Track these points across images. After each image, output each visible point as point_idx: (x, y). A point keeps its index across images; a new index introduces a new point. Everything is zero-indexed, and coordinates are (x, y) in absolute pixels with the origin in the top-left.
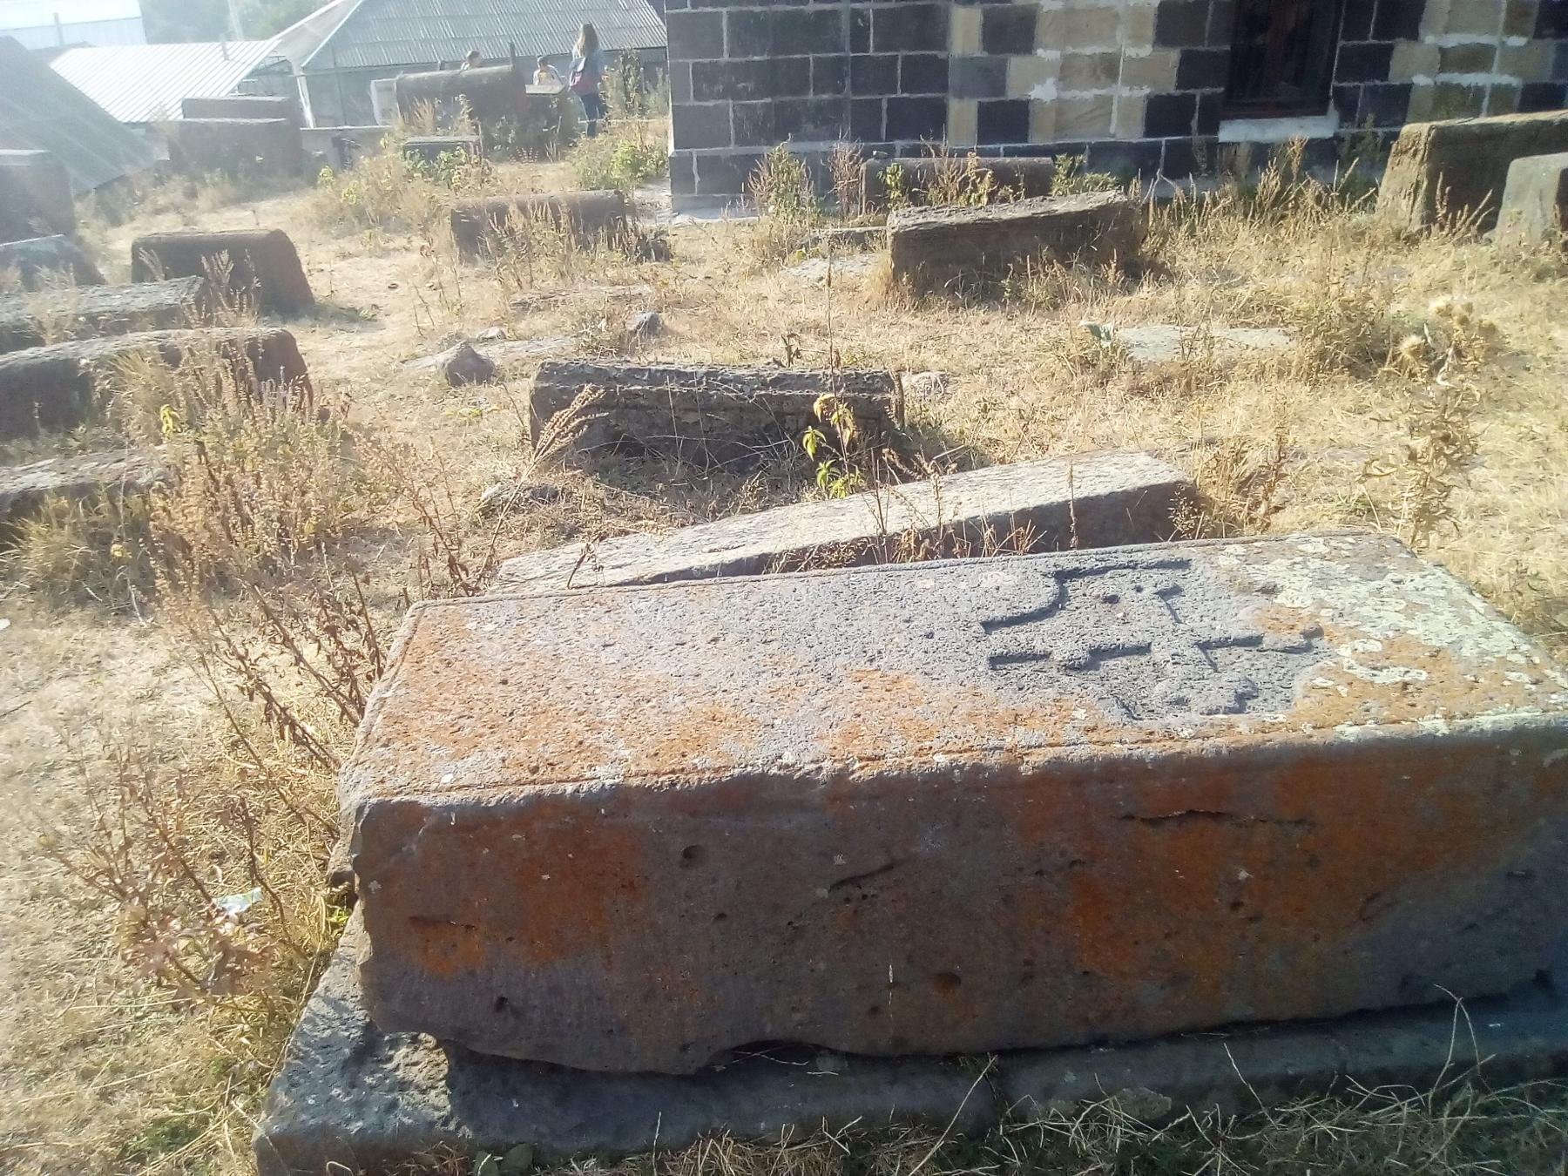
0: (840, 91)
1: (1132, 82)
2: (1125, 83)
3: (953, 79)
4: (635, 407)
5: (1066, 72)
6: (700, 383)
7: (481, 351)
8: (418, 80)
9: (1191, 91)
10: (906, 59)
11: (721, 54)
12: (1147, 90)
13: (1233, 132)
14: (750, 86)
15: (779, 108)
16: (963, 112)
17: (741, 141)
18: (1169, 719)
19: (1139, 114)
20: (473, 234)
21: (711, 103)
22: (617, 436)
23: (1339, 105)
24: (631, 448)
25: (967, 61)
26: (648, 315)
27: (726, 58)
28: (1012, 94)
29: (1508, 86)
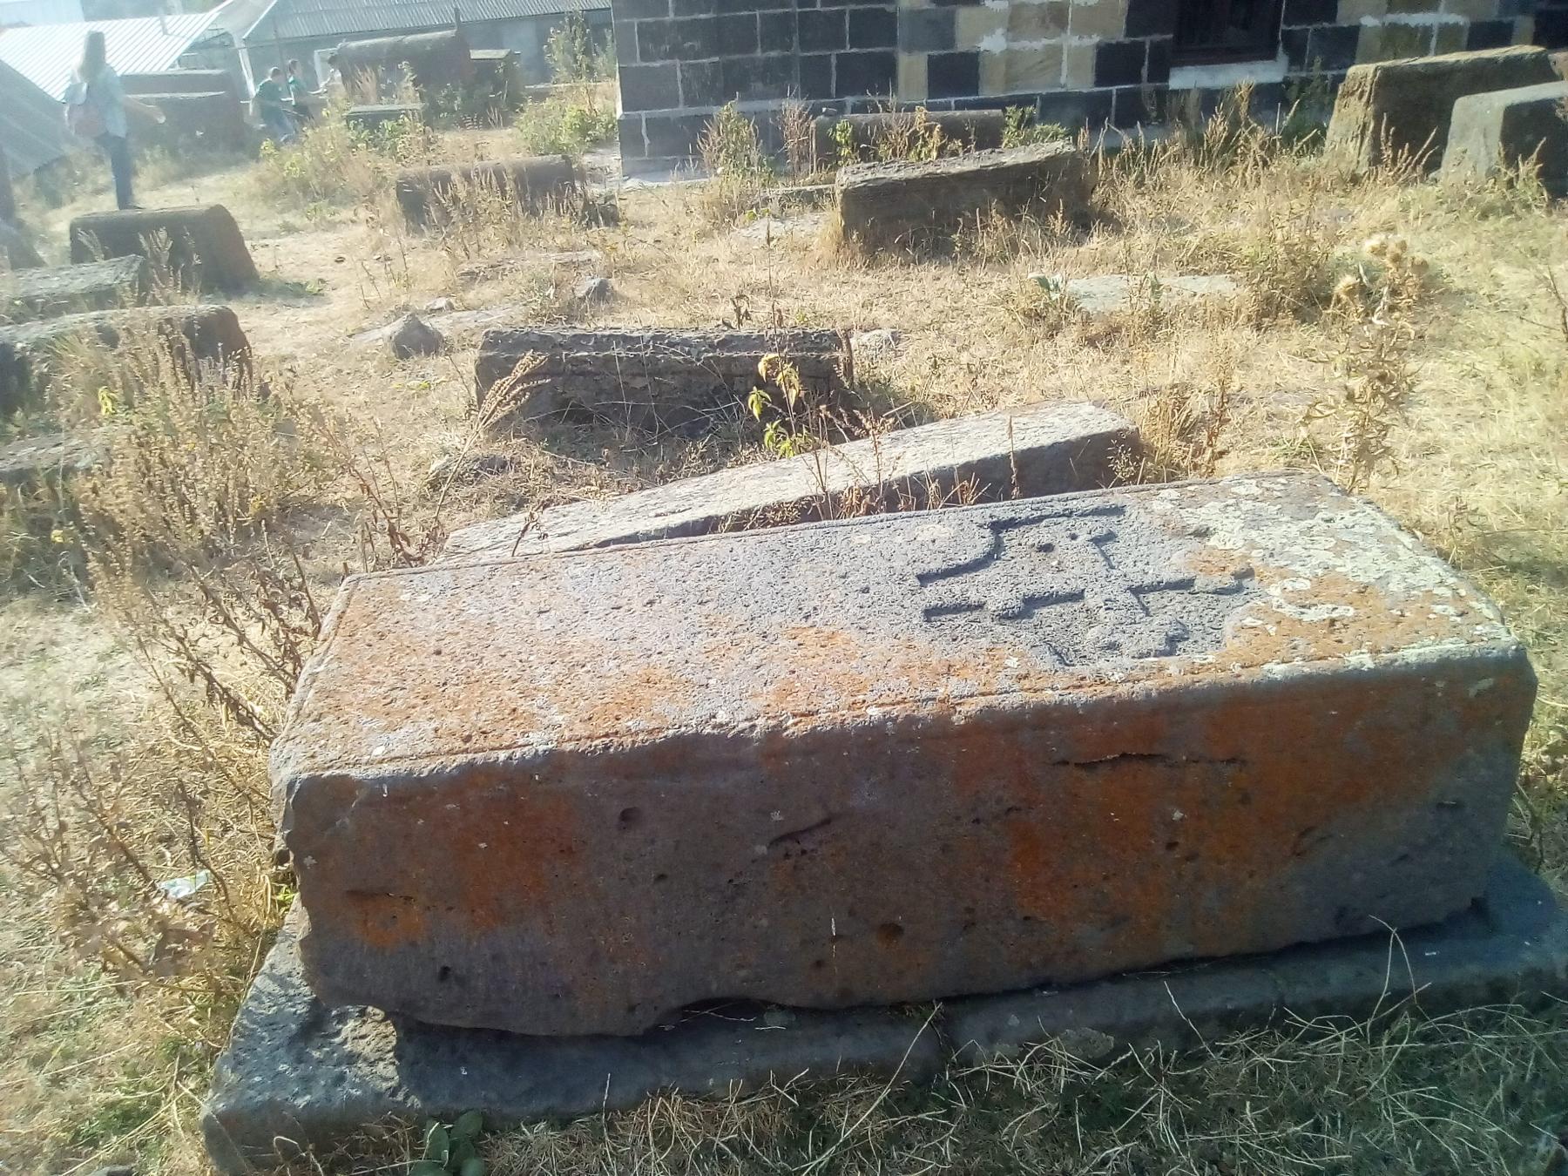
0: (788, 48)
1: (1081, 31)
2: (1074, 32)
3: (901, 32)
4: (583, 373)
5: (1015, 22)
6: (647, 347)
7: (428, 322)
8: (360, 48)
9: (1140, 39)
10: (853, 14)
11: (666, 12)
12: (1096, 39)
13: (1181, 79)
14: (697, 44)
15: (728, 67)
16: (912, 66)
17: (690, 101)
18: (1101, 664)
19: (1090, 61)
20: (418, 204)
21: (657, 64)
22: (566, 402)
23: (1287, 48)
24: (580, 416)
25: (916, 14)
26: (597, 281)
27: (671, 17)
28: (962, 46)
29: (1456, 25)
